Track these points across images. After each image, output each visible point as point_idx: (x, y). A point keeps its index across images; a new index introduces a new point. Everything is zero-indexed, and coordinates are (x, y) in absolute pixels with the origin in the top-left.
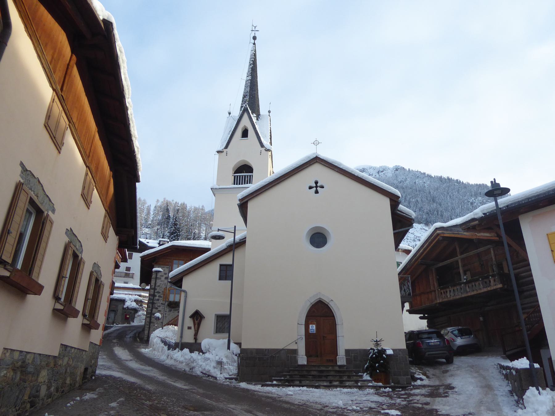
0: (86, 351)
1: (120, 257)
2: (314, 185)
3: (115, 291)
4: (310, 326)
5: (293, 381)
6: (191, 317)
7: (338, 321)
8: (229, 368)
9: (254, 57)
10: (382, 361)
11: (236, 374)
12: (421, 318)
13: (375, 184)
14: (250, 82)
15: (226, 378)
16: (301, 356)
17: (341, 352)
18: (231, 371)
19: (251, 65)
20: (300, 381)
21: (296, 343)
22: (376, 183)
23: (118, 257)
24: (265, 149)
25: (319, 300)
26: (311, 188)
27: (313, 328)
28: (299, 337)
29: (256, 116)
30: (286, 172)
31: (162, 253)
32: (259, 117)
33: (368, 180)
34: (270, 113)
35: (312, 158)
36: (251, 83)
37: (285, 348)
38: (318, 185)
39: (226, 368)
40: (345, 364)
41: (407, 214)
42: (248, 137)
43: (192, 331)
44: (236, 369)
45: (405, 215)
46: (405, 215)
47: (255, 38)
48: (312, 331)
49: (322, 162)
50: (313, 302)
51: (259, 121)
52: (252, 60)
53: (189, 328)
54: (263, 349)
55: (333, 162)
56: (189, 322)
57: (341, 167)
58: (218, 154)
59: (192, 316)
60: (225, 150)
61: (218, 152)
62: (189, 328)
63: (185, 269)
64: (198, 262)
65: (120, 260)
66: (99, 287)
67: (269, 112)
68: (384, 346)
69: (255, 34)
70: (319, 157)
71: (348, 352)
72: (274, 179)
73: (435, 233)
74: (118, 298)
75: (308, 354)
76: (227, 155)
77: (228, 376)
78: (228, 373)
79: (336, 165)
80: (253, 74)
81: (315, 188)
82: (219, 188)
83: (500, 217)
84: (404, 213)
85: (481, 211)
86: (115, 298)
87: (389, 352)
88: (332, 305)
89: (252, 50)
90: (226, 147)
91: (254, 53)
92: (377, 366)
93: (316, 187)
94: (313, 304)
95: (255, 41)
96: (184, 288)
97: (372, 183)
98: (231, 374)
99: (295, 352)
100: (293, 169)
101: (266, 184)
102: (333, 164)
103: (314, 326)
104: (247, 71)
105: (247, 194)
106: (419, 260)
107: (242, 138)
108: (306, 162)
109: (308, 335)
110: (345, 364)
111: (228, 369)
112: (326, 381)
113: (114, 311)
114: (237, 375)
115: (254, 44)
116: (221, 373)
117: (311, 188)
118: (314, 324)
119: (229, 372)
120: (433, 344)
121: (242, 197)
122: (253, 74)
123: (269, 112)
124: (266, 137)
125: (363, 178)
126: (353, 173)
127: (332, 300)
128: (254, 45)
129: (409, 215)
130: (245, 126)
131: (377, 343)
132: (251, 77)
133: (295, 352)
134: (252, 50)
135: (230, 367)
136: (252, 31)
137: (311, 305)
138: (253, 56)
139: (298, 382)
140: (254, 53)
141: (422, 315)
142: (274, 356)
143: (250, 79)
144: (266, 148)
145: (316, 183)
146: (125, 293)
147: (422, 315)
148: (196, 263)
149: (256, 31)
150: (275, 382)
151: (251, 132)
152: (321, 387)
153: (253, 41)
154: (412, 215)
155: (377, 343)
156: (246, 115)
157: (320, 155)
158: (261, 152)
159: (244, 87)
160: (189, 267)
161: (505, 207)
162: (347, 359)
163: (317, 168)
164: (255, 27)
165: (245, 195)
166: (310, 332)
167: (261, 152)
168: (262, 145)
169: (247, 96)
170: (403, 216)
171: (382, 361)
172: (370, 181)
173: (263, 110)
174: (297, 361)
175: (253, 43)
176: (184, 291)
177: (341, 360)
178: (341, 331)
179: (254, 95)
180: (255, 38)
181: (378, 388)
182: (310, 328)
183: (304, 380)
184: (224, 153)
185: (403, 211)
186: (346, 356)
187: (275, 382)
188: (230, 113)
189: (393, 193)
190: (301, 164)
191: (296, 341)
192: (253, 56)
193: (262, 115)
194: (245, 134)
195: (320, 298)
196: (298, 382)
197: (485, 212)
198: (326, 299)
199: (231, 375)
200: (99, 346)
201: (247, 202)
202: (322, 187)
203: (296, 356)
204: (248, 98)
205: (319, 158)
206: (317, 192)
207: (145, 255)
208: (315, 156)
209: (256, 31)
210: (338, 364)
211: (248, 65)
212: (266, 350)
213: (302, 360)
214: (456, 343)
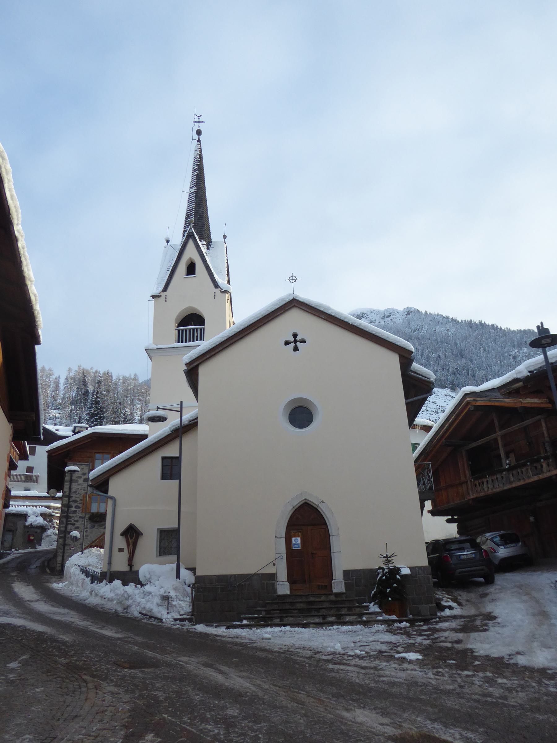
1: (17, 453)
2: (292, 339)
3: (11, 503)
4: (294, 539)
5: (271, 618)
6: (122, 534)
7: (332, 530)
8: (180, 604)
9: (199, 160)
10: (395, 585)
11: (189, 613)
12: (448, 521)
13: (377, 334)
14: (195, 195)
15: (176, 620)
16: (281, 583)
18: (183, 609)
19: (195, 171)
20: (281, 620)
21: (274, 565)
22: (379, 333)
23: (15, 453)
24: (220, 291)
25: (304, 502)
26: (287, 343)
27: (297, 541)
28: (278, 556)
29: (205, 243)
30: (251, 323)
32: (210, 245)
33: (367, 330)
34: (226, 238)
36: (197, 197)
37: (258, 572)
38: (298, 338)
39: (175, 605)
40: (344, 590)
41: (424, 375)
42: (195, 275)
43: (125, 555)
44: (190, 606)
45: (420, 376)
46: (420, 376)
47: (199, 133)
48: (296, 546)
49: (302, 305)
50: (296, 506)
51: (211, 251)
52: (197, 165)
53: (121, 550)
54: (227, 575)
55: (317, 306)
56: (120, 542)
57: (329, 312)
58: (154, 300)
59: (124, 534)
60: (163, 294)
61: (154, 297)
62: (121, 550)
63: (112, 466)
64: (130, 455)
65: (17, 457)
67: (225, 237)
69: (199, 127)
70: (297, 299)
71: (347, 574)
72: (234, 333)
73: (463, 401)
74: (17, 511)
75: (291, 579)
76: (166, 301)
77: (179, 617)
78: (179, 612)
79: (322, 309)
80: (199, 184)
81: (293, 344)
82: (157, 349)
83: (551, 376)
84: (420, 375)
85: (527, 368)
86: (12, 512)
87: (406, 571)
88: (323, 508)
89: (196, 150)
90: (165, 290)
91: (200, 153)
92: (388, 591)
93: (295, 342)
94: (296, 508)
95: (200, 136)
96: (111, 493)
97: (374, 333)
98: (182, 613)
99: (272, 577)
100: (261, 317)
101: (224, 339)
102: (318, 308)
103: (299, 539)
104: (190, 180)
105: (197, 356)
106: (443, 440)
107: (187, 275)
108: (279, 306)
111: (178, 606)
112: (318, 616)
113: (10, 531)
114: (190, 614)
115: (199, 141)
116: (168, 613)
117: (287, 343)
118: (298, 537)
119: (180, 610)
120: (465, 557)
121: (190, 360)
122: (199, 184)
123: (225, 237)
124: (221, 273)
125: (361, 327)
126: (346, 320)
127: (322, 502)
128: (199, 143)
129: (427, 376)
130: (190, 259)
132: (196, 188)
133: (272, 577)
134: (196, 150)
135: (181, 603)
136: (195, 122)
137: (294, 509)
138: (198, 158)
139: (279, 620)
140: (200, 153)
141: (450, 517)
142: (243, 584)
143: (195, 192)
144: (222, 289)
145: (295, 336)
146: (27, 504)
147: (450, 517)
149: (201, 122)
150: (245, 622)
151: (199, 266)
152: (311, 625)
153: (196, 137)
154: (431, 377)
155: (388, 560)
157: (298, 296)
158: (215, 295)
160: (118, 463)
162: (346, 584)
163: (295, 314)
164: (199, 117)
165: (194, 357)
166: (293, 549)
167: (215, 295)
168: (216, 285)
169: (192, 215)
170: (419, 378)
171: (395, 585)
172: (370, 331)
173: (215, 235)
174: (275, 590)
176: (112, 498)
178: (336, 544)
179: (201, 214)
180: (199, 133)
181: (391, 623)
182: (294, 542)
183: (287, 617)
184: (162, 299)
187: (245, 622)
188: (169, 240)
189: (403, 346)
190: (273, 310)
191: (274, 562)
192: (198, 158)
193: (215, 242)
194: (191, 269)
195: (305, 499)
196: (279, 620)
197: (532, 369)
198: (314, 500)
199: (182, 615)
201: (197, 367)
202: (303, 341)
203: (275, 583)
205: (298, 301)
206: (296, 349)
207: (54, 449)
208: (291, 298)
209: (201, 122)
210: (335, 591)
212: (231, 576)
214: (498, 554)
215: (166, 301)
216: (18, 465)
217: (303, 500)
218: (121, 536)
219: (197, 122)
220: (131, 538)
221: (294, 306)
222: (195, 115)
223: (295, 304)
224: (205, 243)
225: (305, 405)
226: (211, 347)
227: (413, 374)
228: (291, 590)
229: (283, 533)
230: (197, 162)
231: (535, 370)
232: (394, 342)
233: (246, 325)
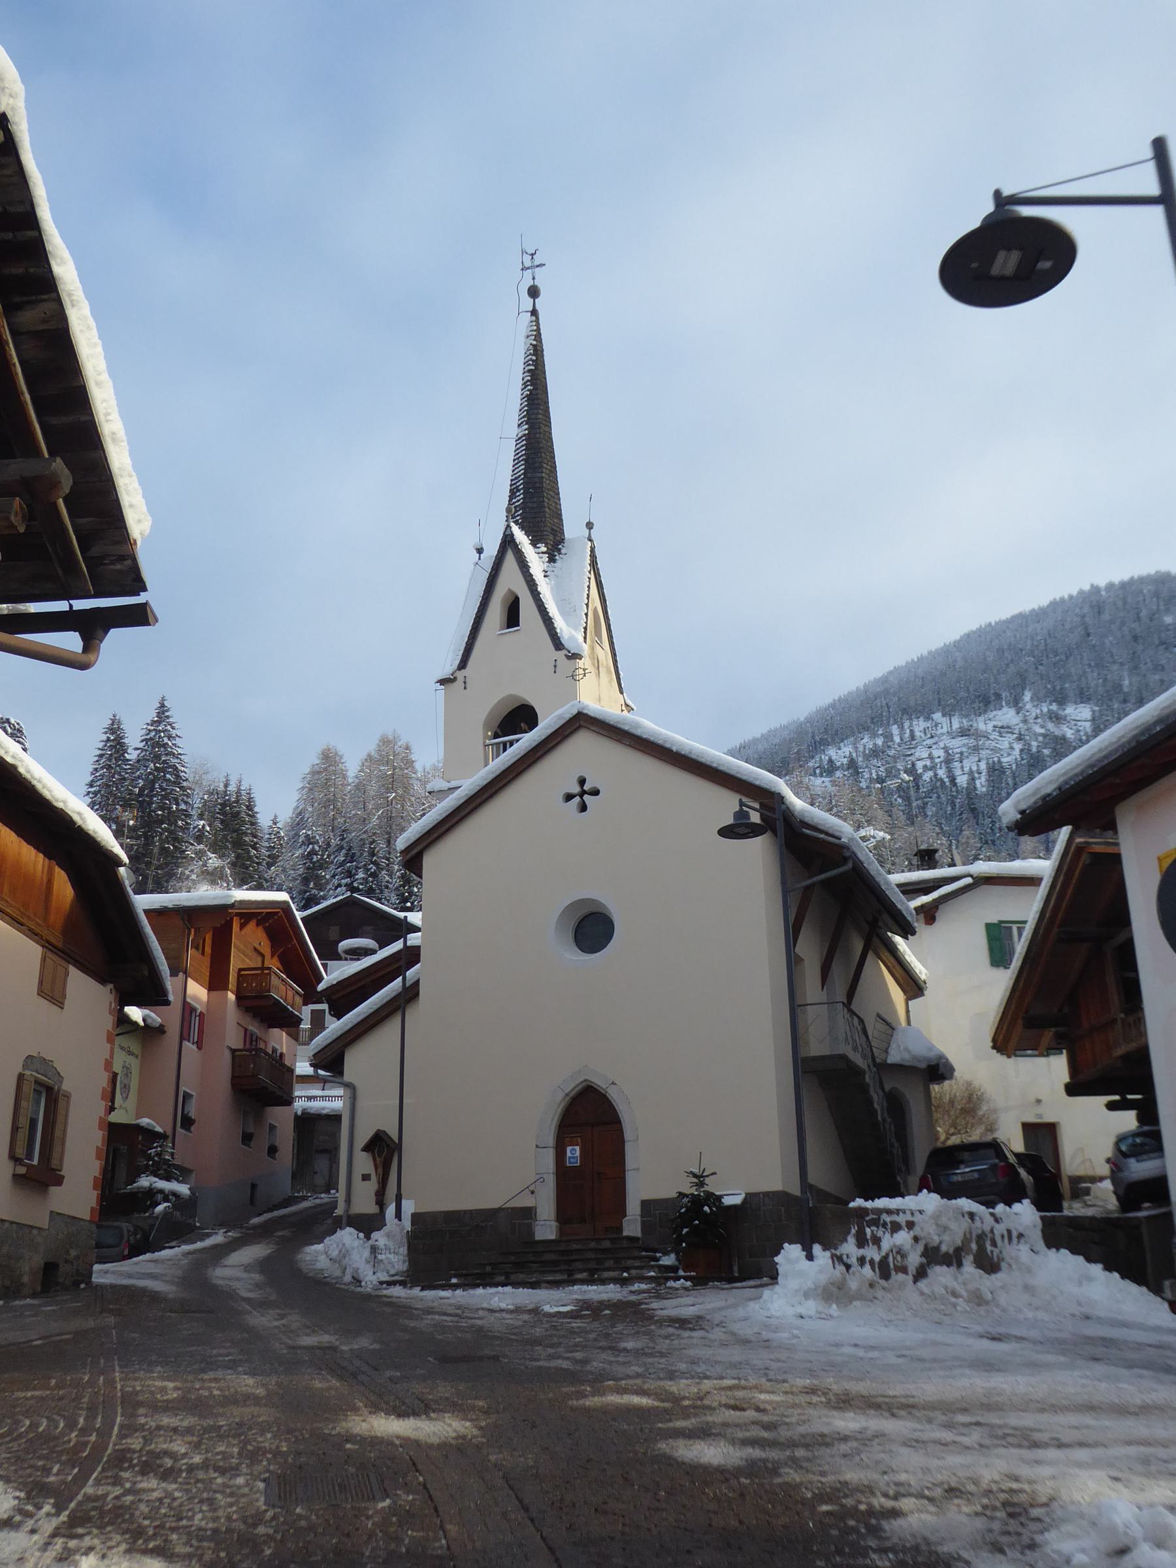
0: (40, 1229)
2: (576, 789)
3: (297, 1093)
4: (569, 1149)
5: (491, 1275)
6: (367, 1148)
7: (628, 1135)
8: (387, 1258)
9: (534, 358)
10: (697, 1222)
11: (404, 1272)
12: (1111, 1106)
13: (721, 768)
14: (524, 442)
15: (381, 1283)
16: (542, 1223)
17: (633, 1208)
19: (525, 385)
20: (507, 1277)
21: (533, 1192)
22: (723, 765)
23: (290, 993)
24: (566, 655)
26: (569, 797)
27: (574, 1153)
28: (538, 1177)
29: (545, 549)
30: (506, 766)
31: (379, 974)
32: (560, 550)
33: (703, 760)
35: (567, 719)
36: (528, 447)
40: (639, 1235)
41: (830, 831)
43: (373, 1185)
44: (404, 1262)
45: (822, 836)
46: (822, 836)
47: (534, 292)
48: (572, 1160)
49: (592, 724)
50: (570, 1092)
51: (558, 564)
52: (529, 371)
53: (366, 1177)
56: (364, 1163)
57: (638, 732)
58: (443, 687)
59: (367, 1148)
60: (460, 675)
61: (442, 682)
62: (366, 1177)
64: (375, 1007)
65: (299, 1000)
66: (56, 1101)
67: (590, 526)
68: (712, 1186)
69: (534, 279)
70: (585, 712)
71: (646, 1205)
72: (478, 788)
74: (333, 1110)
76: (465, 688)
77: (386, 1278)
78: (388, 1273)
79: (626, 728)
80: (533, 417)
81: (586, 797)
82: (450, 789)
83: (850, 865)
84: (821, 831)
86: (324, 1112)
87: (733, 1200)
88: (613, 1094)
89: (528, 337)
90: (463, 665)
91: (535, 343)
93: (582, 793)
94: (572, 1094)
96: (348, 1076)
98: (392, 1272)
99: (528, 1213)
100: (523, 753)
101: (461, 802)
103: (578, 1148)
104: (519, 407)
105: (417, 836)
106: (1056, 930)
108: (553, 730)
109: (563, 1172)
110: (639, 1235)
111: (385, 1261)
112: (561, 1271)
113: (324, 1151)
115: (534, 312)
116: (374, 1273)
117: (569, 797)
118: (577, 1145)
119: (389, 1267)
121: (408, 844)
122: (533, 417)
123: (590, 526)
125: (693, 756)
126: (667, 745)
127: (613, 1083)
128: (534, 318)
129: (837, 834)
130: (510, 592)
131: (700, 1179)
133: (528, 1213)
134: (528, 337)
135: (391, 1256)
137: (568, 1099)
139: (503, 1278)
140: (535, 343)
141: (1117, 1097)
142: (483, 1224)
143: (524, 435)
144: (569, 652)
147: (1117, 1097)
148: (372, 1011)
149: (538, 266)
150: (454, 1281)
151: (527, 608)
152: (543, 1285)
153: (528, 303)
154: (842, 835)
155: (700, 1179)
156: (510, 557)
158: (555, 666)
159: (512, 463)
161: (1055, 790)
162: (643, 1224)
163: (583, 743)
164: (532, 255)
165: (413, 839)
167: (555, 666)
168: (558, 644)
169: (519, 490)
171: (697, 1222)
172: (708, 763)
173: (572, 528)
175: (531, 309)
176: (349, 1086)
177: (632, 1226)
178: (634, 1156)
179: (538, 485)
180: (534, 292)
181: (662, 1281)
182: (569, 1154)
184: (459, 683)
185: (820, 827)
186: (642, 1216)
187: (454, 1281)
188: (482, 549)
190: (543, 737)
191: (531, 1188)
194: (512, 618)
195: (586, 1080)
196: (503, 1278)
197: (1023, 806)
198: (600, 1083)
199: (393, 1276)
200: (90, 1221)
201: (419, 856)
202: (595, 792)
204: (520, 496)
205: (586, 715)
206: (583, 808)
207: (333, 985)
208: (575, 712)
209: (538, 266)
210: (625, 1233)
211: (520, 387)
212: (465, 1212)
213: (546, 1229)
215: (465, 688)
216: (302, 1017)
217: (582, 1082)
218: (365, 1153)
219: (528, 268)
220: (380, 1156)
221: (580, 727)
222: (523, 252)
223: (582, 723)
224: (545, 549)
225: (594, 910)
226: (440, 818)
227: (808, 832)
228: (561, 1231)
229: (551, 1140)
230: (529, 365)
231: (1029, 807)
232: (751, 780)
233: (498, 772)
